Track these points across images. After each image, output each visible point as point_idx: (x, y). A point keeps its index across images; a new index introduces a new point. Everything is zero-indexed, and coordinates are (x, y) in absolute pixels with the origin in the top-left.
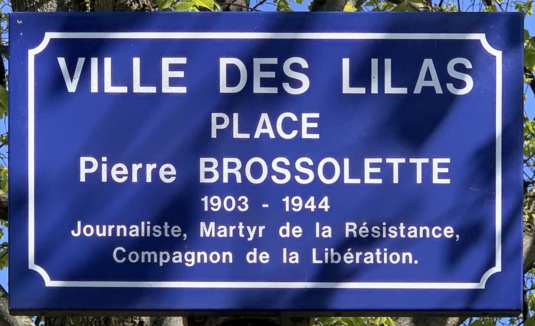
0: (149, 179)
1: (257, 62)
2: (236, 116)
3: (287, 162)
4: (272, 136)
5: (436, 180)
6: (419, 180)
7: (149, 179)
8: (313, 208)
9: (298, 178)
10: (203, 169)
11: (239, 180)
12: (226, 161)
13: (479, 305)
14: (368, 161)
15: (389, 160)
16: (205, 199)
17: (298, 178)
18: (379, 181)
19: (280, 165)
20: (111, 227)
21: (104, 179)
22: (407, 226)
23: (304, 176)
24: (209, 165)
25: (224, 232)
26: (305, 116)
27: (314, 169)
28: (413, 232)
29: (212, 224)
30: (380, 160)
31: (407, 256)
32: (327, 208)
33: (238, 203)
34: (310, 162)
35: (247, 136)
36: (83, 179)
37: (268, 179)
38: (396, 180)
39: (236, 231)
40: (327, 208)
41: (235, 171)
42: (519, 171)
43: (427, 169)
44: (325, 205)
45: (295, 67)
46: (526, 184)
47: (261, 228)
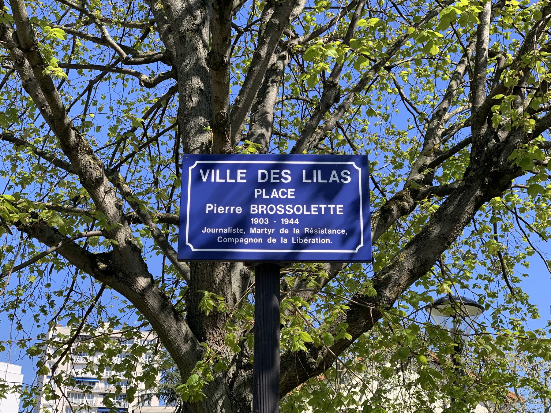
0: (232, 212)
1: (272, 171)
2: (264, 190)
3: (283, 206)
4: (277, 197)
5: (338, 213)
6: (332, 213)
7: (232, 212)
8: (292, 223)
9: (287, 212)
10: (252, 209)
11: (265, 213)
12: (260, 206)
13: (354, 259)
14: (313, 206)
15: (320, 206)
16: (252, 219)
17: (287, 212)
18: (317, 213)
19: (280, 207)
20: (217, 229)
21: (215, 212)
22: (328, 229)
23: (289, 211)
24: (254, 207)
25: (259, 231)
26: (289, 190)
27: (293, 209)
28: (330, 232)
29: (255, 229)
30: (317, 206)
31: (328, 241)
32: (298, 223)
33: (265, 221)
34: (291, 206)
35: (268, 197)
36: (207, 212)
37: (276, 212)
38: (323, 213)
39: (264, 231)
40: (298, 223)
41: (264, 209)
42: (368, 208)
43: (335, 209)
44: (297, 221)
45: (286, 173)
46: (371, 213)
47: (273, 230)
